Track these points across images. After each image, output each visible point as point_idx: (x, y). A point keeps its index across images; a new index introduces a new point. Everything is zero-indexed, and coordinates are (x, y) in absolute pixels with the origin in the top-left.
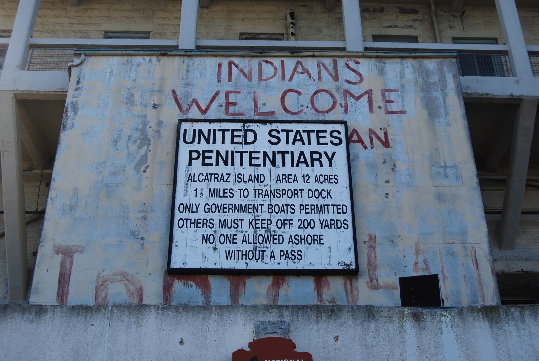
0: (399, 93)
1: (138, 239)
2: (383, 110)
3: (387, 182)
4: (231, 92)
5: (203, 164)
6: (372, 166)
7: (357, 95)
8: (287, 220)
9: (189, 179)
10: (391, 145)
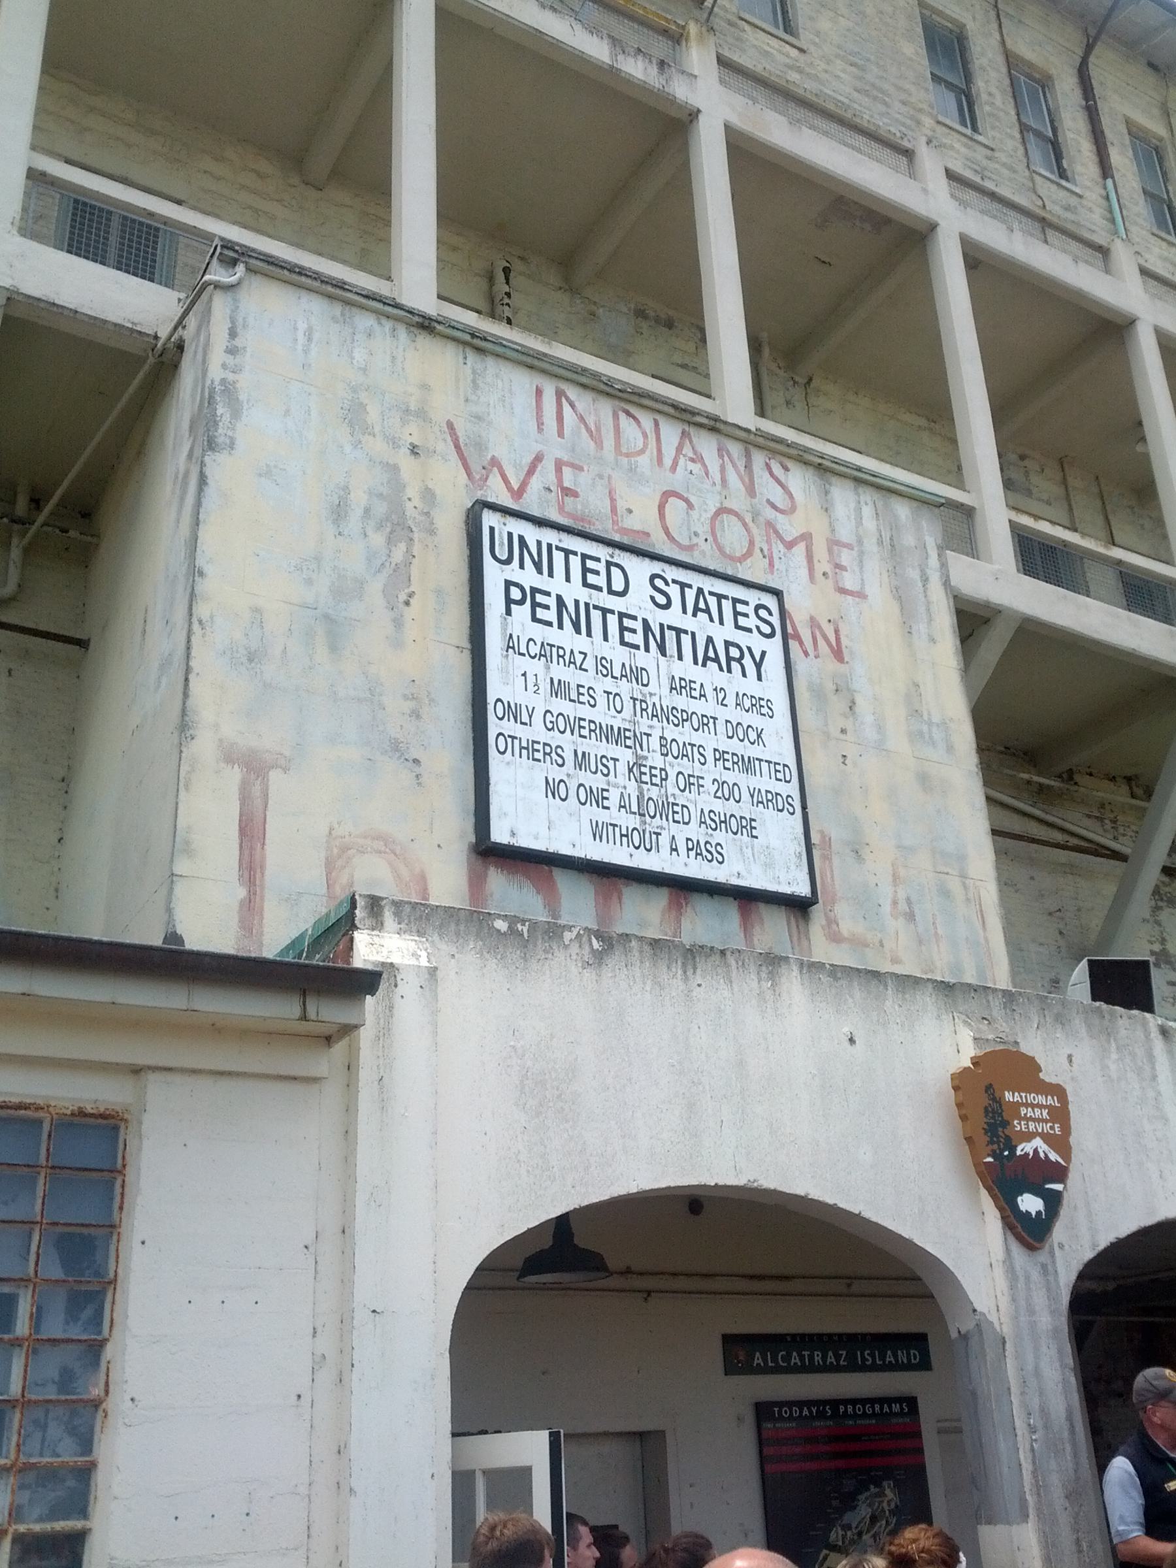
1: (406, 760)
2: (830, 583)
3: (843, 731)
7: (788, 538)
9: (509, 647)
10: (846, 660)
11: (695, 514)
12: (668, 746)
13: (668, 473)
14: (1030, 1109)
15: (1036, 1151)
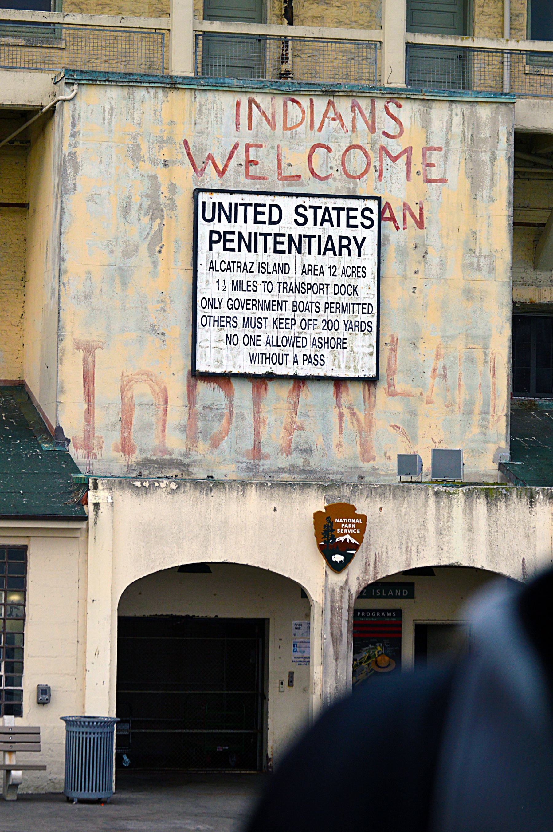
0: (442, 153)
2: (421, 177)
3: (416, 273)
4: (252, 146)
5: (225, 249)
6: (402, 252)
7: (394, 155)
8: (311, 320)
9: (210, 268)
11: (332, 155)
12: (297, 306)
13: (317, 133)
14: (346, 525)
15: (346, 540)
